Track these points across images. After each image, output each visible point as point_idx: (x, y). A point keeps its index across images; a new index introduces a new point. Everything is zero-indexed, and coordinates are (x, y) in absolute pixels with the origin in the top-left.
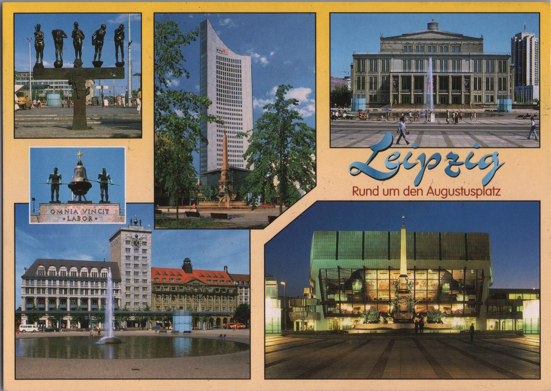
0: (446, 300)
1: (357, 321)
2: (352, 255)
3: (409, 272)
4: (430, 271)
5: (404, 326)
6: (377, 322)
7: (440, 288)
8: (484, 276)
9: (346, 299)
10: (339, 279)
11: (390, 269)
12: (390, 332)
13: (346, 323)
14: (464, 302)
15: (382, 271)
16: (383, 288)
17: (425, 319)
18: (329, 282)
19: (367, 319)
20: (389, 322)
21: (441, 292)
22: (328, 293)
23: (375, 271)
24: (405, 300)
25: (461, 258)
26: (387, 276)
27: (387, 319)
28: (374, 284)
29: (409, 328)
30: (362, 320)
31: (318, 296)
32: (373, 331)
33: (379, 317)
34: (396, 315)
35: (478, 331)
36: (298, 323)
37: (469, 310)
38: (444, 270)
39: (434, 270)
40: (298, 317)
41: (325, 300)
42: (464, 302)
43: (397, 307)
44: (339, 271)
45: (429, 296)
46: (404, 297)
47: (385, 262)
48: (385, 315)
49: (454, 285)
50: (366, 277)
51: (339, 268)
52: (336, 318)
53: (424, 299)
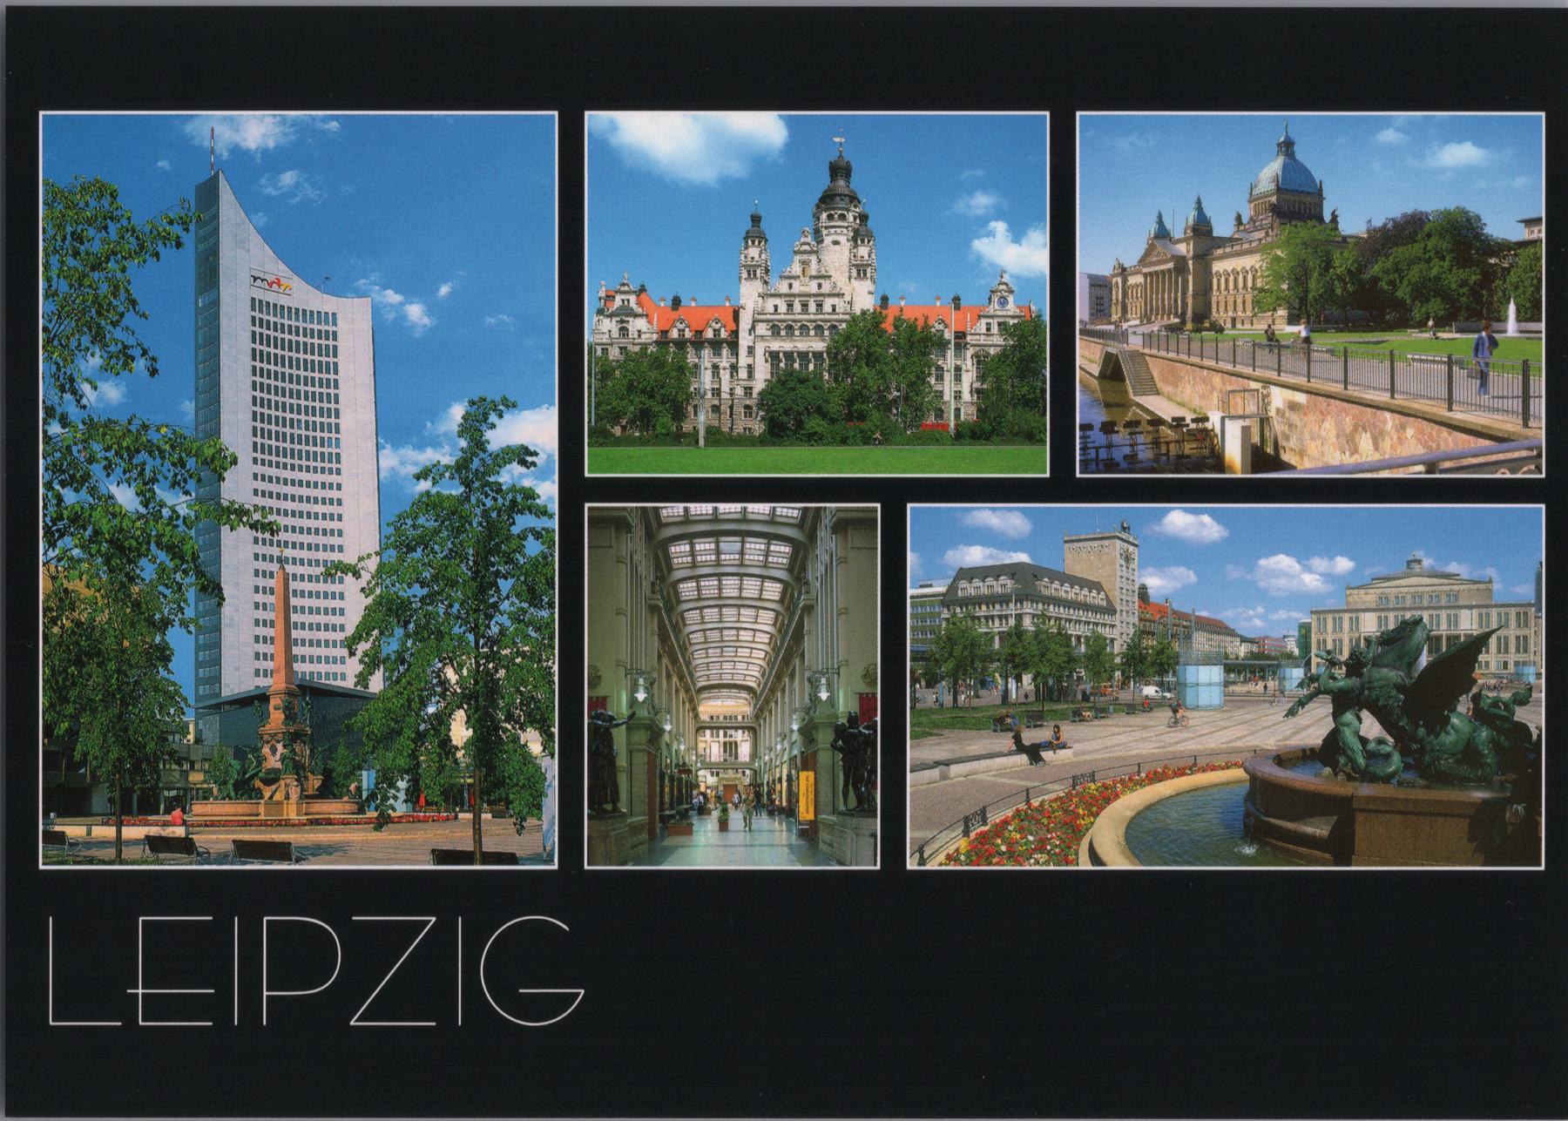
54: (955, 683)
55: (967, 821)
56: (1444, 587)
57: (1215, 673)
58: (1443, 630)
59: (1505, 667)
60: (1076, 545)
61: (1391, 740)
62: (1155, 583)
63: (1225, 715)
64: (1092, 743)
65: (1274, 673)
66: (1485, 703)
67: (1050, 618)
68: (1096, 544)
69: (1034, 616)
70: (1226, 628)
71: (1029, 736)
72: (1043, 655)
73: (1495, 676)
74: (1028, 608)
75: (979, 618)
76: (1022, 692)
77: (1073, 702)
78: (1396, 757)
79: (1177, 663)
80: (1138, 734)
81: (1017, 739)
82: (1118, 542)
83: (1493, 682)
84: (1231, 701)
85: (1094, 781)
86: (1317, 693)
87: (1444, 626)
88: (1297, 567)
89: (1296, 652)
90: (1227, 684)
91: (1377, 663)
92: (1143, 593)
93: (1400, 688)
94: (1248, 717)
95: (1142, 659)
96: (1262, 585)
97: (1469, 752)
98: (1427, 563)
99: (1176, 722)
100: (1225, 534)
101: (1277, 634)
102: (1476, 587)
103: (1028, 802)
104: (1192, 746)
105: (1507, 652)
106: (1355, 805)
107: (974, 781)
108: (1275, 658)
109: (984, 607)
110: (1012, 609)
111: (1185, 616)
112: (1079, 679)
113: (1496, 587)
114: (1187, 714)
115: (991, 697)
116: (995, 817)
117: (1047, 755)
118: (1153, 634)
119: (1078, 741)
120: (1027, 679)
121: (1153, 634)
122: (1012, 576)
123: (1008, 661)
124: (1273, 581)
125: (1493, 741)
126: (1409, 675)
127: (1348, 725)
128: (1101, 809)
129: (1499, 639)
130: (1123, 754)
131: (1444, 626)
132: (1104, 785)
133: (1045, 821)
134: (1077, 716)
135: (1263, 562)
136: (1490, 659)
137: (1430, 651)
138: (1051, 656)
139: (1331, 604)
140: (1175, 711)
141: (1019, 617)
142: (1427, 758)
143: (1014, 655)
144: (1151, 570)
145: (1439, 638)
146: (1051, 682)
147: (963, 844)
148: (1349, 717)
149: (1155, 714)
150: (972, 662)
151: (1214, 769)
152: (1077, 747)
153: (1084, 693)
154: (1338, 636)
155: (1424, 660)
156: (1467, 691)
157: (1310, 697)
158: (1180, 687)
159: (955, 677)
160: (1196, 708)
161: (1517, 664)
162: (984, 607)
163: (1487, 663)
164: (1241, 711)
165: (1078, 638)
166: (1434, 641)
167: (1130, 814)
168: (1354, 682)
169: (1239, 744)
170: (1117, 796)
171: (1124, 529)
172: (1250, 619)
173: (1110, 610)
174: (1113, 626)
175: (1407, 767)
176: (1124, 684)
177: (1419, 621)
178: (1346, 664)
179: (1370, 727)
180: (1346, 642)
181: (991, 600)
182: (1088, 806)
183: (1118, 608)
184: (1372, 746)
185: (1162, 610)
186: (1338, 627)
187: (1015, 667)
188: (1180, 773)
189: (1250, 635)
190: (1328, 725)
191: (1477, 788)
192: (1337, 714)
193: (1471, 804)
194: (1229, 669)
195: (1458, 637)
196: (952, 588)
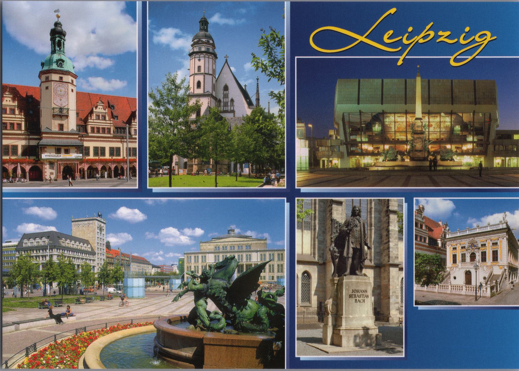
54: (22, 287)
55: (27, 349)
56: (244, 242)
57: (141, 282)
58: (244, 262)
59: (273, 279)
60: (77, 223)
61: (220, 312)
62: (113, 240)
63: (146, 301)
64: (85, 314)
65: (168, 282)
66: (263, 296)
67: (65, 257)
68: (86, 222)
69: (58, 256)
70: (146, 261)
71: (56, 311)
72: (62, 274)
73: (268, 283)
74: (55, 252)
75: (33, 257)
76: (52, 291)
77: (76, 295)
78: (223, 320)
79: (123, 277)
80: (107, 310)
81: (50, 312)
82: (96, 222)
83: (267, 285)
84: (148, 295)
86: (187, 291)
87: (244, 260)
88: (178, 233)
89: (178, 272)
90: (146, 286)
93: (225, 289)
94: (156, 302)
96: (162, 241)
97: (256, 319)
98: (237, 231)
99: (123, 304)
102: (259, 242)
103: (55, 341)
104: (131, 315)
105: (273, 272)
106: (205, 342)
107: (31, 331)
108: (168, 275)
109: (35, 252)
110: (48, 252)
111: (128, 256)
112: (79, 284)
114: (128, 300)
115: (38, 293)
116: (40, 348)
117: (64, 319)
118: (113, 264)
119: (79, 313)
120: (55, 284)
121: (113, 264)
122: (48, 237)
123: (46, 276)
124: (167, 239)
125: (267, 313)
126: (229, 283)
127: (201, 305)
128: (89, 344)
129: (270, 266)
130: (99, 319)
131: (244, 260)
132: (90, 334)
133: (63, 350)
135: (163, 231)
136: (266, 276)
137: (238, 272)
138: (66, 274)
139: (193, 250)
140: (122, 299)
141: (51, 256)
142: (237, 321)
143: (49, 274)
144: (111, 234)
145: (242, 266)
146: (65, 286)
147: (25, 360)
148: (201, 302)
149: (113, 301)
150: (30, 277)
151: (141, 326)
152: (78, 315)
153: (81, 291)
154: (196, 265)
155: (236, 276)
156: (255, 290)
159: (22, 283)
160: (133, 298)
161: (278, 277)
162: (35, 252)
163: (265, 277)
164: (152, 299)
165: (78, 266)
166: (240, 267)
170: (96, 338)
171: (99, 216)
172: (156, 257)
173: (93, 253)
174: (94, 260)
175: (228, 325)
176: (99, 287)
177: (233, 258)
178: (200, 277)
179: (212, 306)
180: (200, 267)
181: (38, 248)
183: (97, 252)
184: (212, 315)
185: (117, 253)
187: (49, 279)
188: (125, 327)
190: (192, 305)
191: (261, 334)
192: (196, 300)
193: (257, 341)
194: (147, 280)
195: (251, 265)
196: (21, 243)
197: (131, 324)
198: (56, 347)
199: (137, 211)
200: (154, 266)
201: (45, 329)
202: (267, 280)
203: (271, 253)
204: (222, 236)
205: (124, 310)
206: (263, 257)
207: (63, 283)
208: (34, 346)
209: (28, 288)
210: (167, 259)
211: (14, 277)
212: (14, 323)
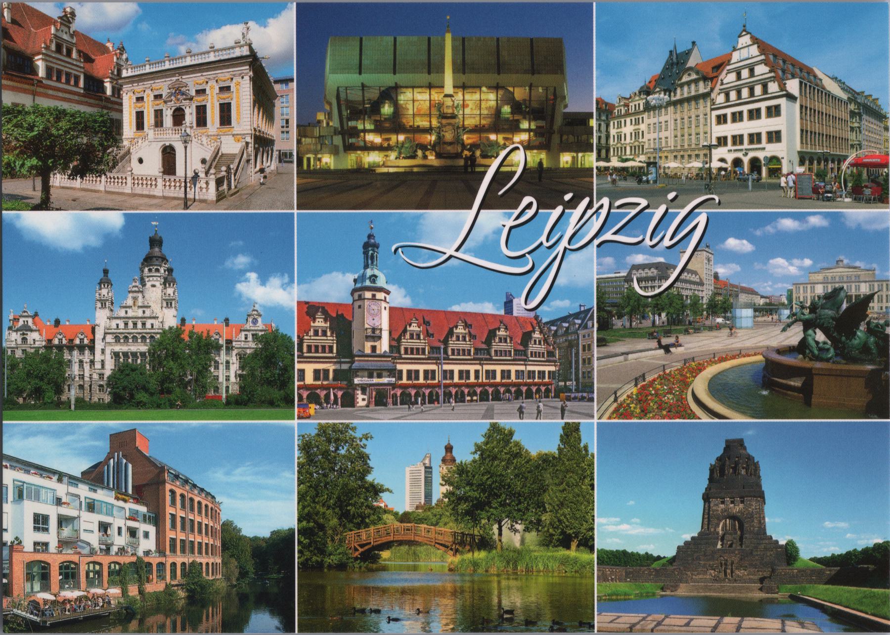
0: (506, 127)
1: (387, 156)
2: (379, 69)
3: (456, 90)
4: (484, 89)
5: (449, 162)
6: (413, 157)
7: (498, 111)
8: (556, 96)
9: (372, 127)
10: (364, 100)
11: (430, 86)
12: (430, 170)
13: (372, 158)
14: (529, 130)
15: (419, 90)
16: (422, 113)
17: (478, 153)
18: (350, 104)
19: (400, 153)
20: (430, 157)
21: (499, 117)
22: (350, 119)
23: (411, 90)
24: (451, 127)
25: (526, 72)
26: (426, 96)
27: (427, 153)
28: (410, 106)
29: (456, 165)
30: (393, 155)
31: (335, 123)
32: (408, 169)
33: (416, 151)
34: (438, 149)
35: (549, 170)
36: (309, 159)
37: (537, 141)
38: (503, 88)
39: (489, 87)
40: (309, 152)
41: (346, 128)
42: (529, 130)
43: (439, 138)
44: (363, 90)
45: (483, 122)
46: (449, 124)
47: (424, 78)
48: (424, 147)
49: (517, 107)
50: (399, 98)
51: (363, 86)
52: (359, 152)
53: (476, 126)
55: (636, 380)
57: (749, 312)
58: (853, 292)
61: (829, 342)
62: (721, 271)
64: (694, 344)
71: (665, 341)
72: (671, 304)
73: (877, 313)
78: (832, 350)
81: (659, 342)
83: (875, 316)
84: (757, 325)
85: (694, 361)
87: (853, 290)
88: (786, 263)
89: (786, 302)
90: (755, 317)
91: (823, 307)
92: (716, 276)
93: (833, 319)
95: (716, 306)
97: (865, 348)
98: (846, 261)
99: (731, 334)
100: (754, 248)
101: (778, 294)
104: (739, 345)
111: (736, 287)
112: (687, 315)
113: (877, 272)
115: (647, 323)
116: (649, 378)
117: (672, 350)
120: (663, 315)
122: (656, 268)
126: (837, 312)
128: (697, 374)
131: (853, 290)
134: (687, 332)
135: (771, 261)
136: (874, 305)
138: (674, 305)
139: (802, 280)
140: (731, 330)
143: (657, 304)
144: (719, 265)
145: (851, 296)
147: (635, 390)
148: (810, 332)
149: (722, 331)
151: (749, 356)
152: (687, 346)
155: (845, 306)
157: (793, 323)
158: (733, 318)
160: (741, 328)
166: (849, 298)
167: (710, 376)
168: (812, 316)
169: (761, 344)
170: (705, 368)
175: (837, 355)
176: (707, 318)
177: (842, 288)
179: (820, 336)
180: (809, 298)
182: (692, 373)
184: (821, 345)
185: (725, 284)
186: (805, 291)
188: (734, 357)
189: (764, 295)
190: (801, 335)
191: (869, 364)
192: (805, 330)
194: (755, 310)
195: (860, 295)
197: (740, 354)
198: (664, 378)
199: (745, 242)
200: (762, 297)
201: (653, 359)
202: (876, 310)
203: (880, 283)
204: (830, 266)
205: (732, 340)
206: (871, 287)
207: (672, 314)
208: (643, 377)
209: (637, 319)
210: (777, 290)
211: (623, 308)
212: (623, 354)
